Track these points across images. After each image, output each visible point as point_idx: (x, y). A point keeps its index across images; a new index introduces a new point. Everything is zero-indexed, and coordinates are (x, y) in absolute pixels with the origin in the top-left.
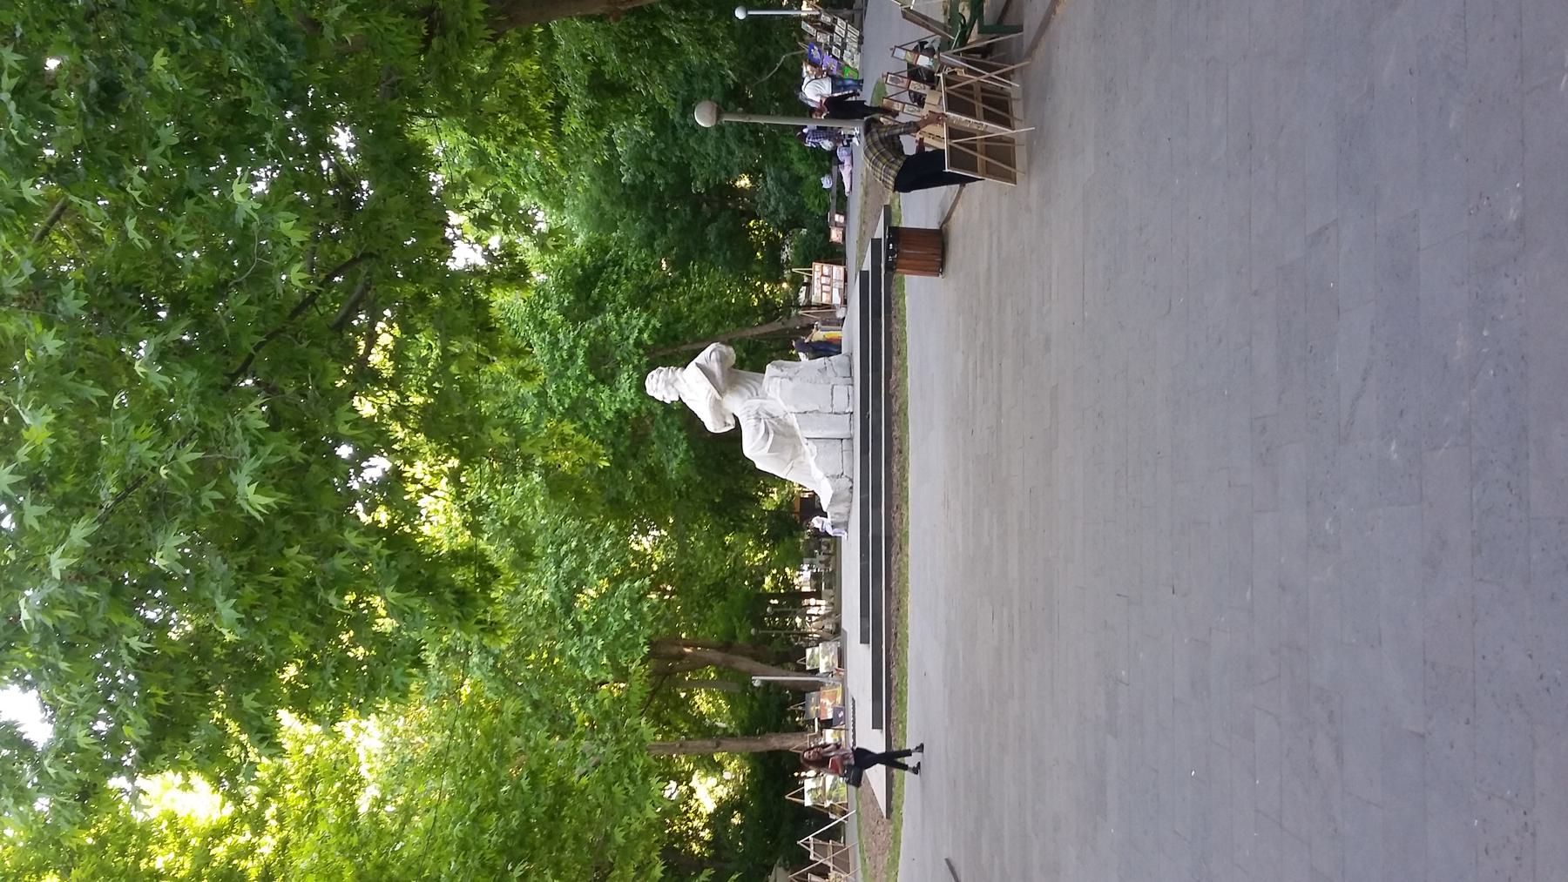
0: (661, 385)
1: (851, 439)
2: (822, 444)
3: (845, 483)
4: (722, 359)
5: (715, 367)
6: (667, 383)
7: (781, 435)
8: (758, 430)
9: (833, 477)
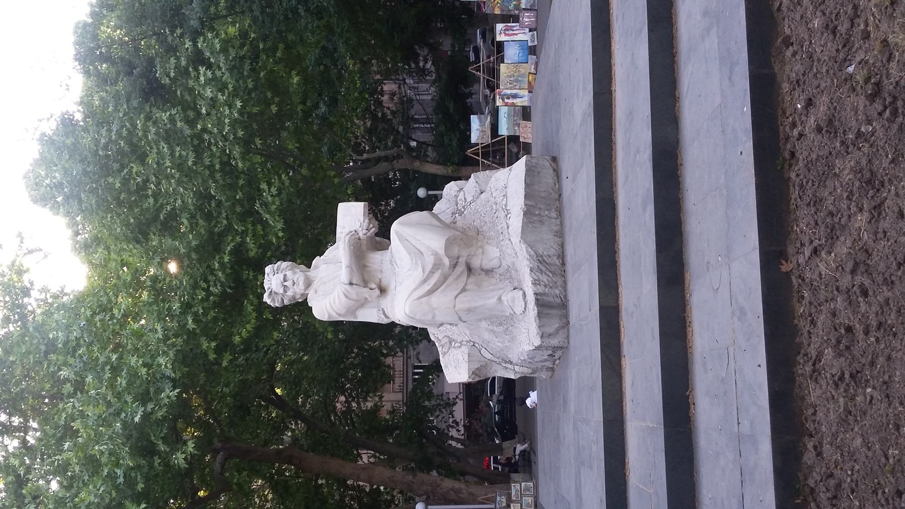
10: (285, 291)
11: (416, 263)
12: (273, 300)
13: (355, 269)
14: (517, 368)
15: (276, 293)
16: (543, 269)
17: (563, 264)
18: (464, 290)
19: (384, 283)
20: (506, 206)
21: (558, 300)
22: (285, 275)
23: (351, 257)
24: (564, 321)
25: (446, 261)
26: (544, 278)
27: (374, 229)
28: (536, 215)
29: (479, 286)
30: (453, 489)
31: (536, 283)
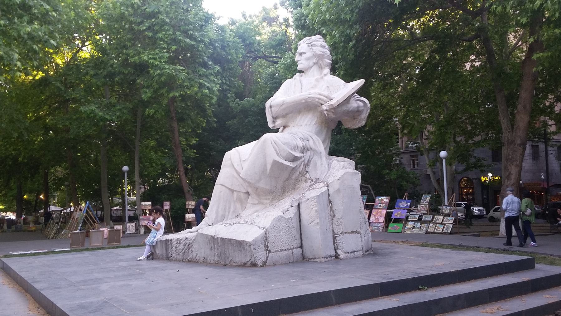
0: (318, 50)
1: (304, 259)
2: (295, 223)
3: (260, 256)
4: (358, 112)
5: (353, 105)
6: (320, 57)
7: (286, 177)
8: (295, 148)
9: (265, 240)
13: (283, 107)
16: (186, 247)
17: (189, 261)
18: (232, 191)
19: (287, 129)
20: (239, 223)
21: (170, 256)
22: (305, 53)
23: (294, 102)
24: (161, 257)
26: (181, 247)
28: (214, 244)
29: (240, 200)
30: (510, 174)
31: (179, 241)
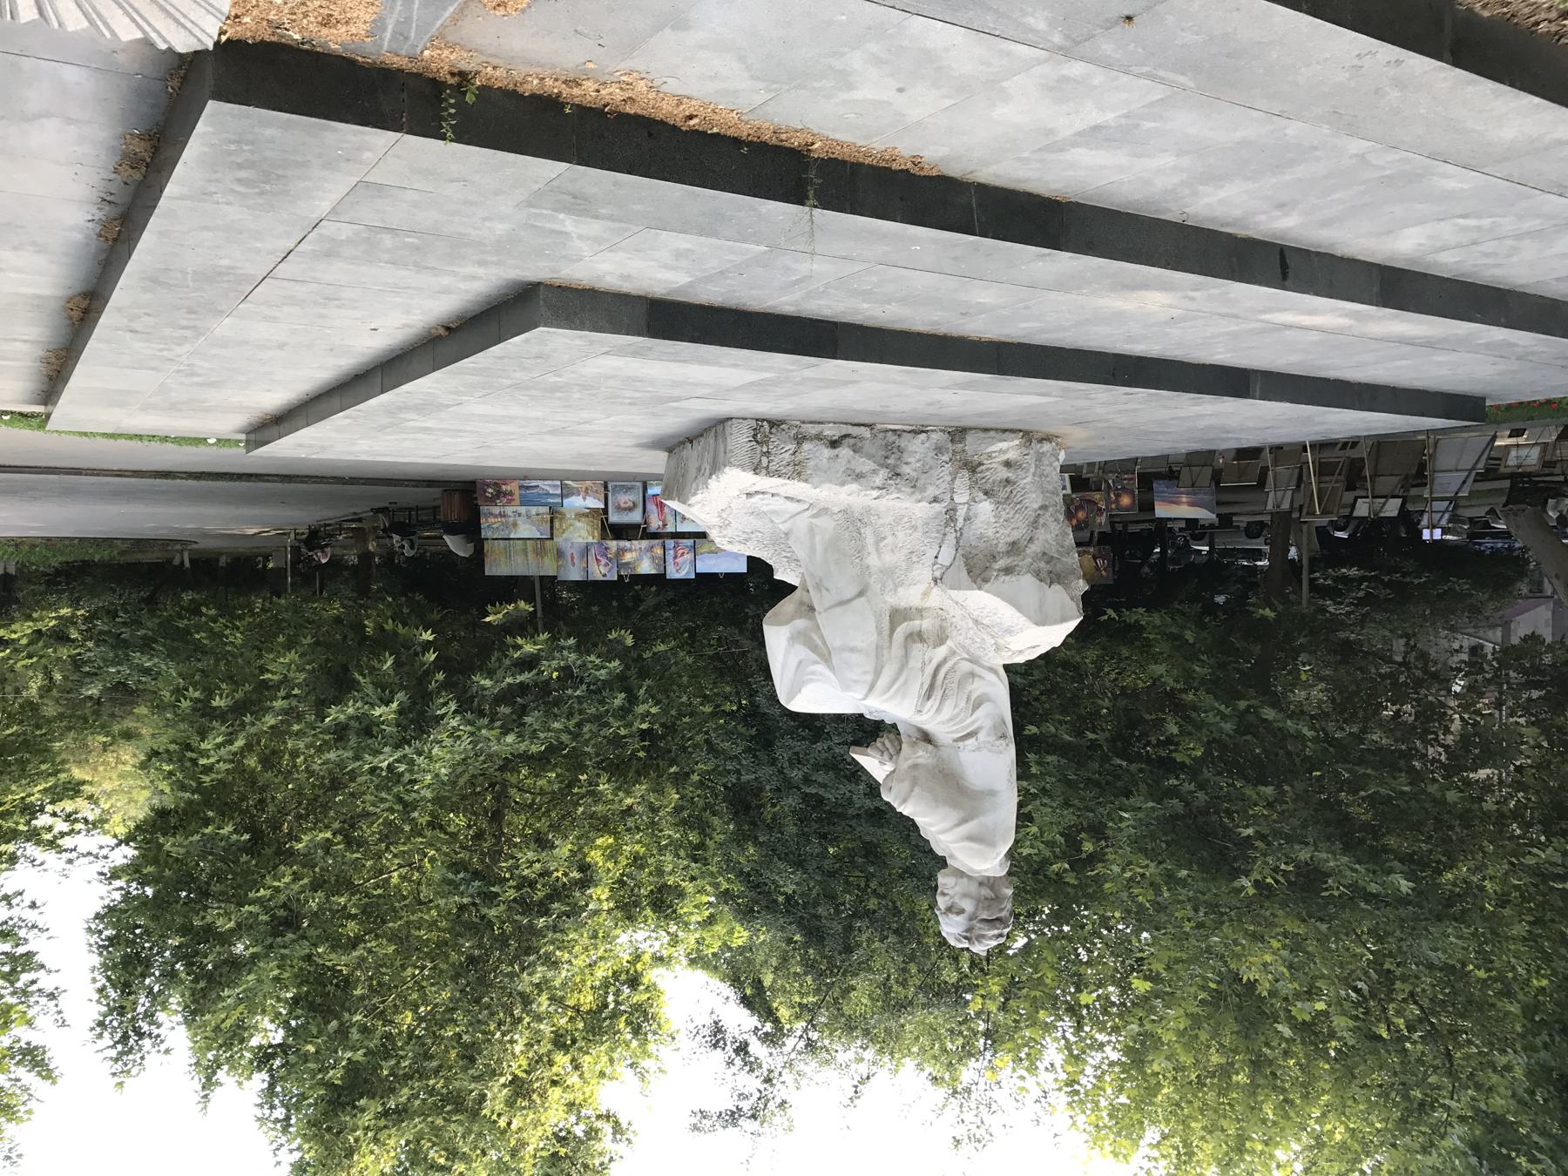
10: (962, 911)
11: (813, 673)
12: (980, 938)
14: (957, 499)
15: (969, 930)
25: (801, 623)
27: (888, 744)
